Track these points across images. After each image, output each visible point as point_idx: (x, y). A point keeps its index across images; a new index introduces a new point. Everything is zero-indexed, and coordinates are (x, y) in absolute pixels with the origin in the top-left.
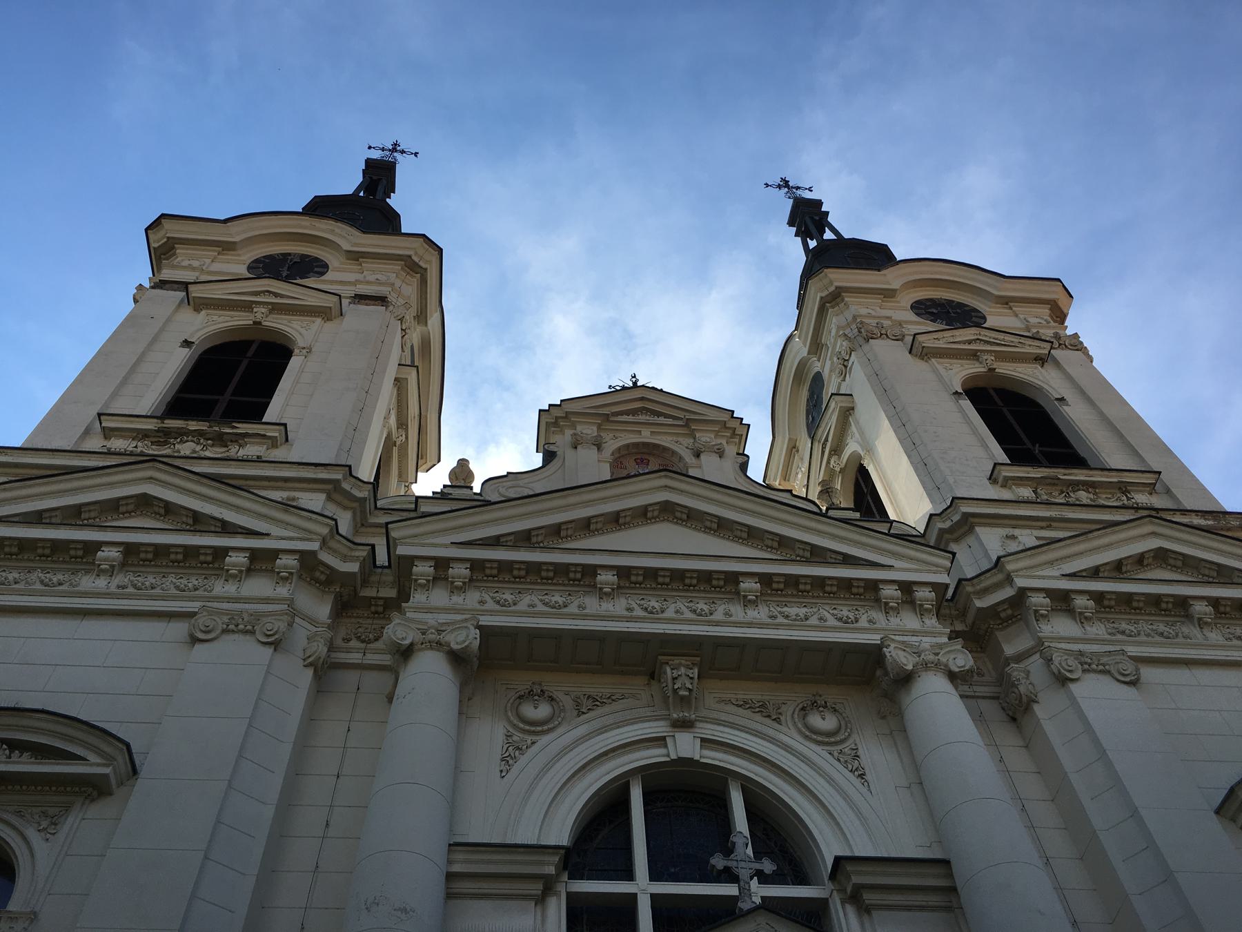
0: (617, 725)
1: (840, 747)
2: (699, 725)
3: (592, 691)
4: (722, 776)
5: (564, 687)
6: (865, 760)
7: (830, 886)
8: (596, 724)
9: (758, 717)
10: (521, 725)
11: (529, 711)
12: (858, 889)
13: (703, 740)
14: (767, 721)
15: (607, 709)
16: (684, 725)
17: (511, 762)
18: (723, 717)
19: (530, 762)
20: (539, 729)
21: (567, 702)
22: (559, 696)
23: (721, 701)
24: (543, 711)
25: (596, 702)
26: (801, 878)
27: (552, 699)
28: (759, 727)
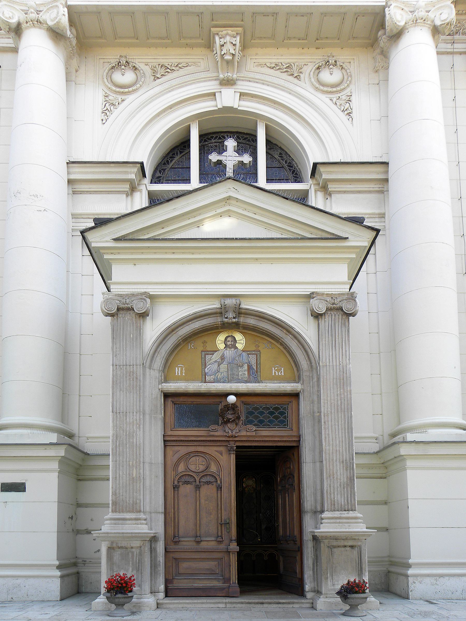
0: (181, 86)
1: (339, 95)
2: (239, 83)
3: (165, 62)
4: (255, 118)
5: (144, 59)
6: (355, 103)
7: (311, 181)
8: (166, 86)
9: (285, 76)
10: (114, 88)
11: (118, 77)
12: (326, 182)
13: (242, 94)
14: (291, 78)
15: (175, 74)
16: (228, 83)
17: (108, 113)
18: (258, 76)
19: (120, 114)
20: (126, 90)
21: (147, 70)
22: (141, 66)
23: (260, 65)
24: (128, 77)
25: (168, 69)
26: (297, 179)
27: (135, 69)
28: (282, 82)
